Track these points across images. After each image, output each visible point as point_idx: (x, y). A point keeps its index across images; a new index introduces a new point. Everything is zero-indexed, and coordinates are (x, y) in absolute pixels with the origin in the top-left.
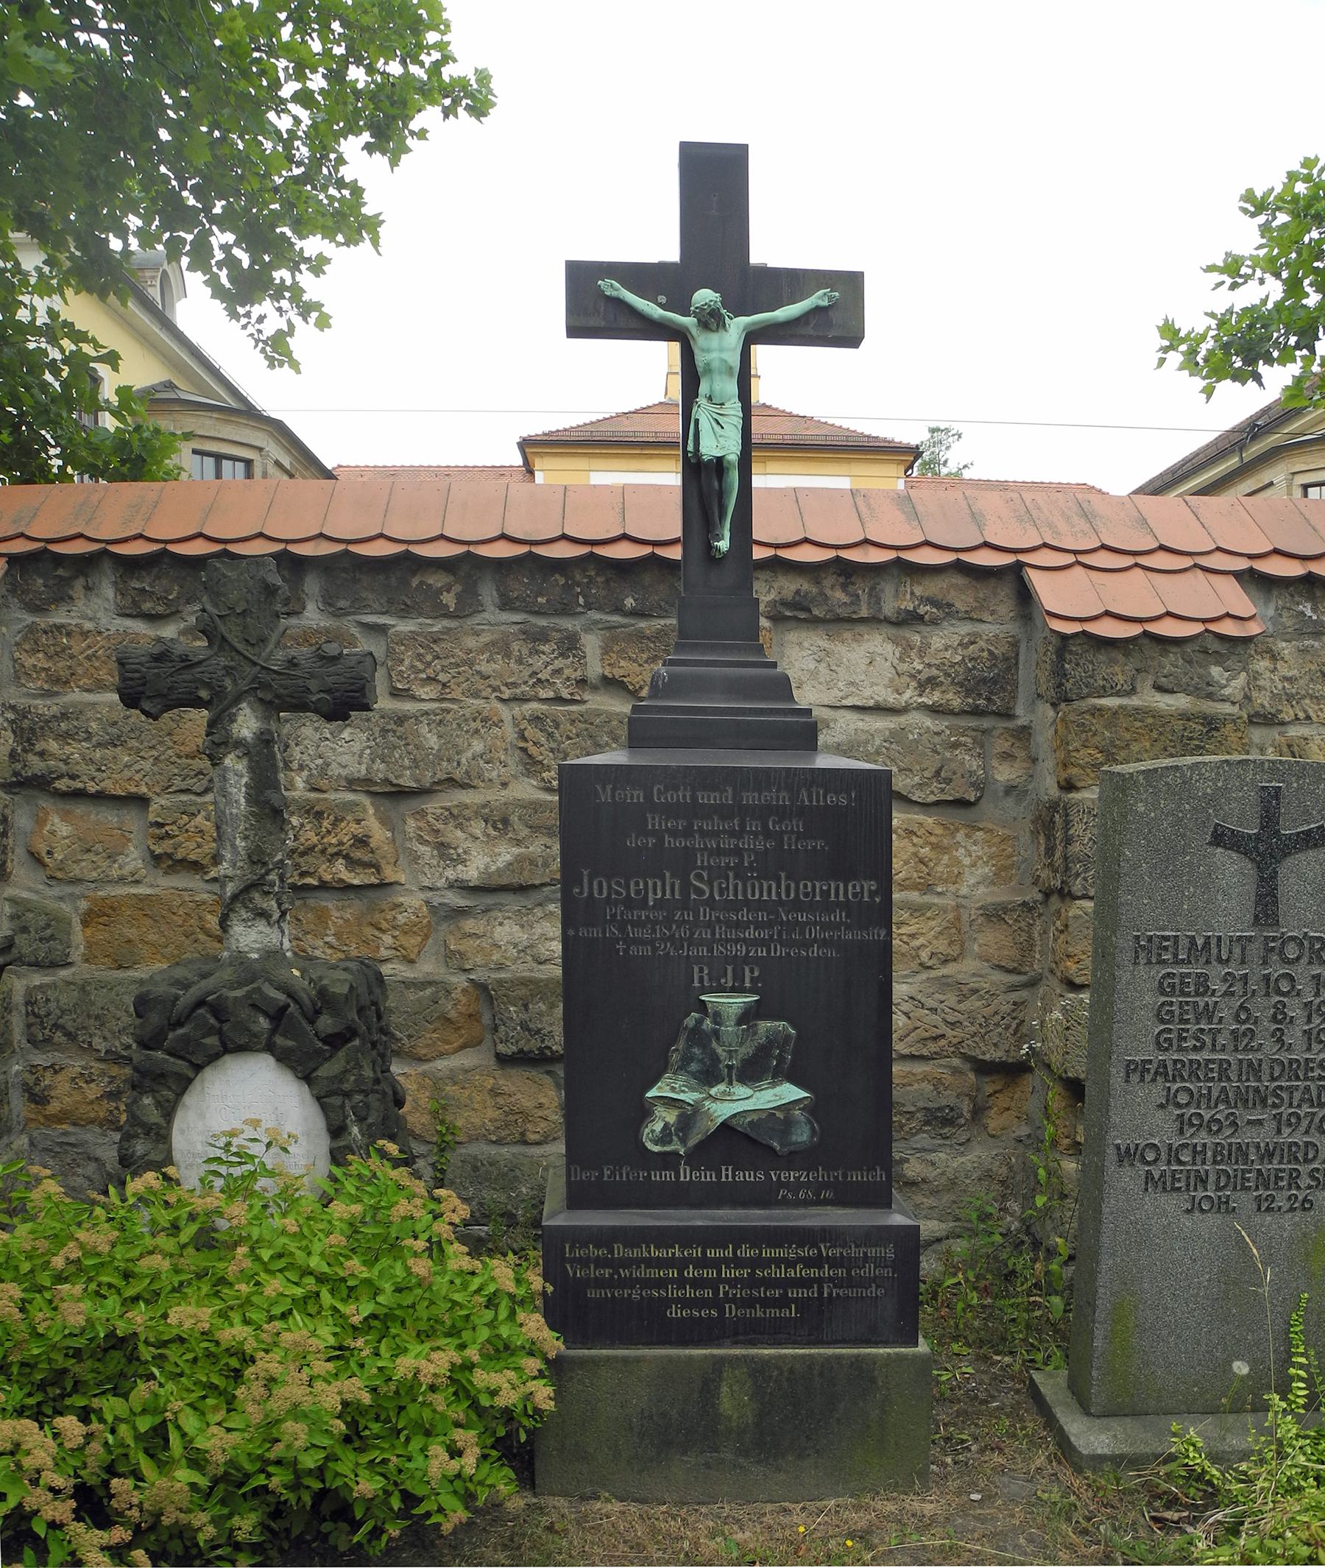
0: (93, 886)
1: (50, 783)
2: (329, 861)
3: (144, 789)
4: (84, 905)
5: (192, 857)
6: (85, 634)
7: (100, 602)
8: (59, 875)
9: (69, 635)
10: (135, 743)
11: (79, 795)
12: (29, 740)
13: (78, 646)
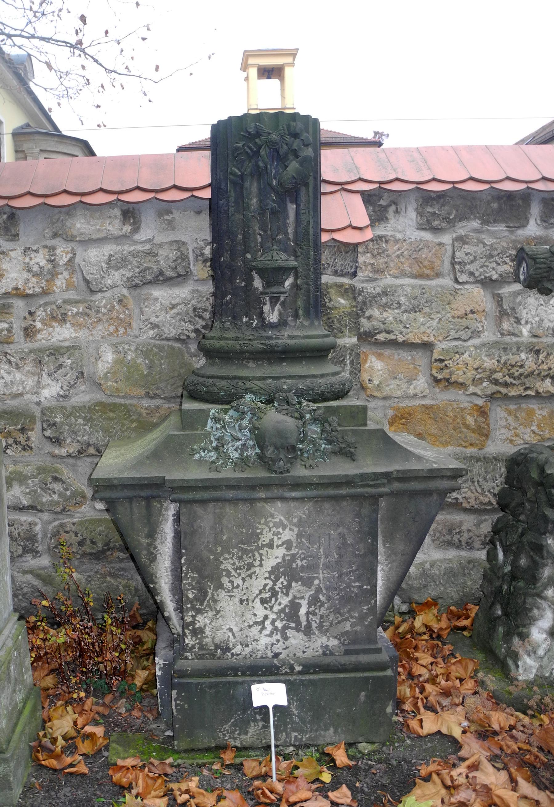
0: (397, 400)
1: (373, 336)
2: (542, 380)
3: (432, 339)
4: (391, 413)
5: (461, 380)
6: (397, 241)
7: (406, 221)
8: (376, 394)
9: (387, 242)
10: (427, 310)
11: (394, 344)
12: (361, 309)
13: (392, 249)
